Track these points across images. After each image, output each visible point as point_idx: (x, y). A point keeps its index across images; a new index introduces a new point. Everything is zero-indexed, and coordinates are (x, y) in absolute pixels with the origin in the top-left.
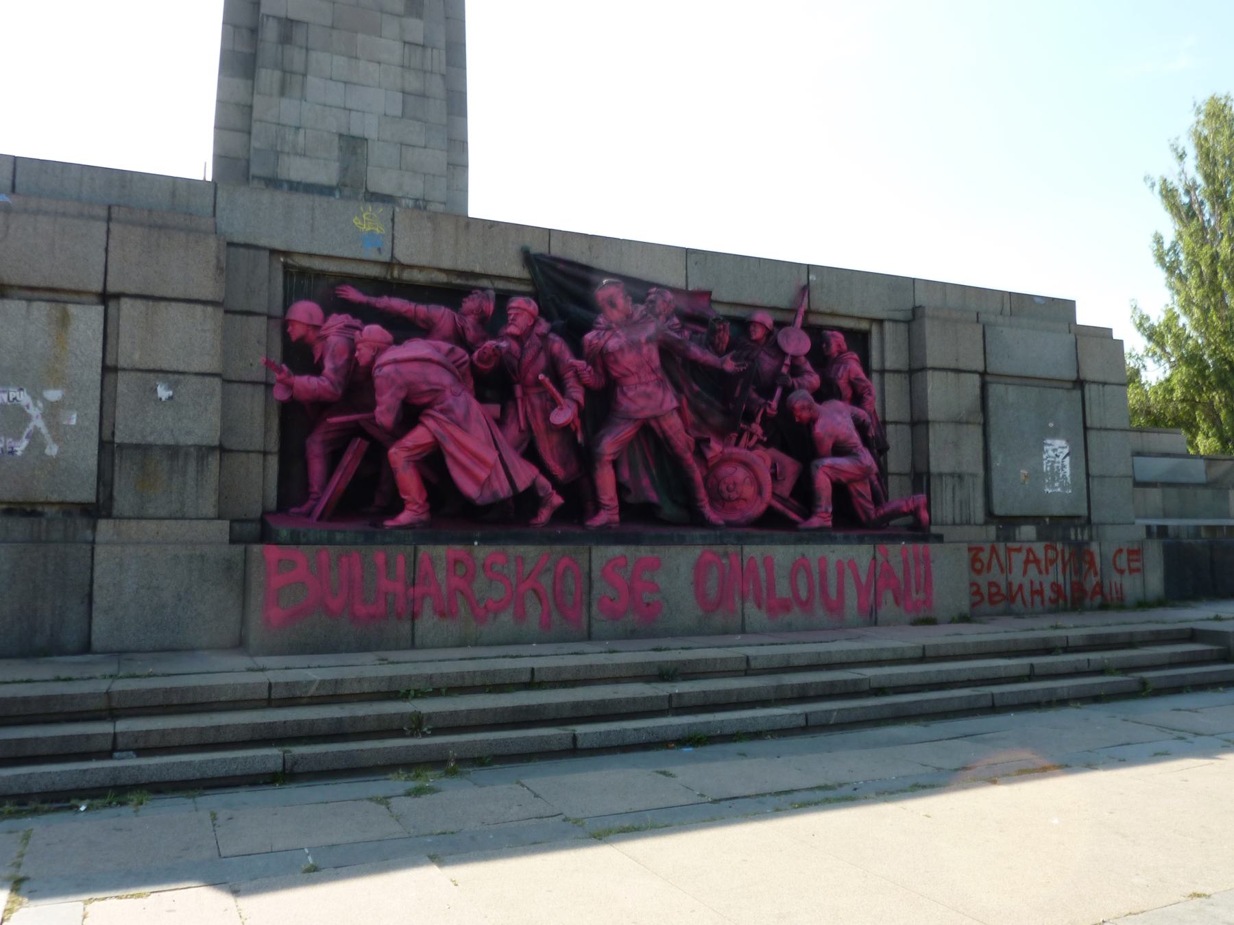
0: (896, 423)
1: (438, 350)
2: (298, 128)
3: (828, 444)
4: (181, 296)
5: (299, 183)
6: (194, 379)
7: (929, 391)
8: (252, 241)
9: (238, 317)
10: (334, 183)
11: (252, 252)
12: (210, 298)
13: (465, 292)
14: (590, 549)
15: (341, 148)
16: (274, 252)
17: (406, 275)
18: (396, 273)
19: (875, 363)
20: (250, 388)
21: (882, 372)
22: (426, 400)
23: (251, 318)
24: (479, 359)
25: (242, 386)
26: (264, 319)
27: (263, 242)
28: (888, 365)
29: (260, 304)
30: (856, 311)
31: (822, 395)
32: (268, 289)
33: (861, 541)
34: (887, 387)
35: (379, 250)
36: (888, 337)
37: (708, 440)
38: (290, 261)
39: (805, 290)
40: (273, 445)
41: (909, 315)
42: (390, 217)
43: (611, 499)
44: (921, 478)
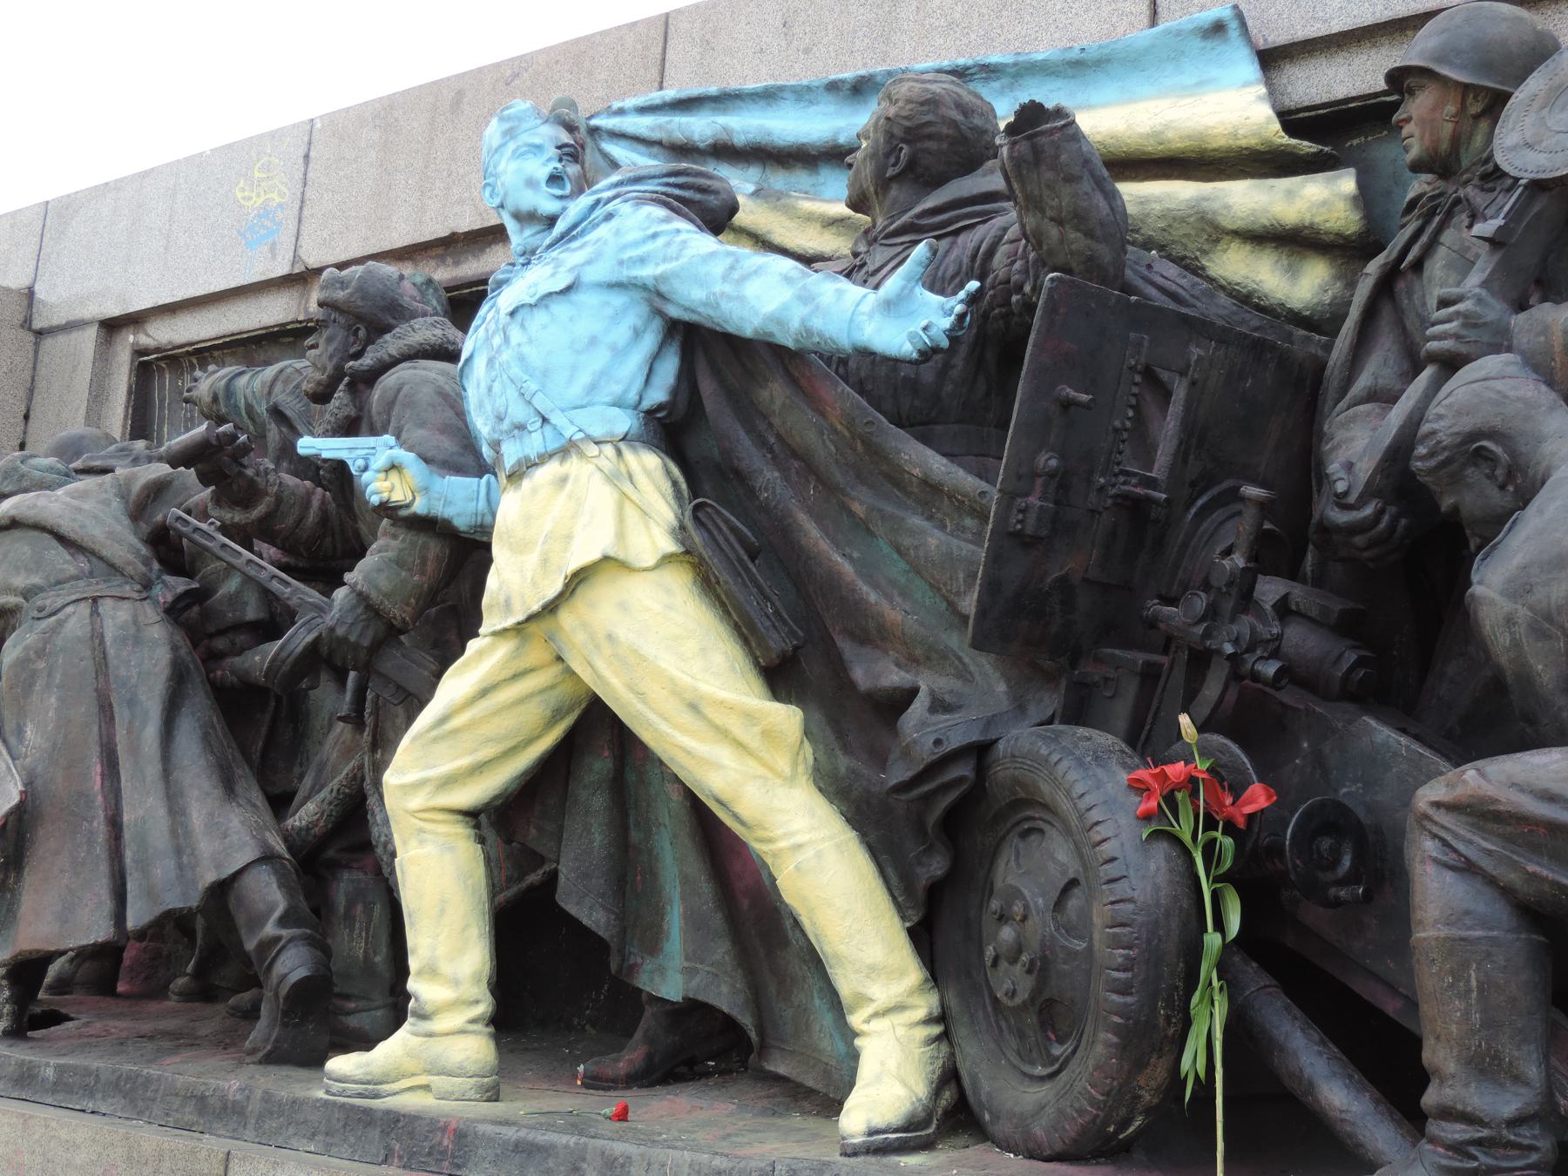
38: (144, 340)
42: (301, 152)
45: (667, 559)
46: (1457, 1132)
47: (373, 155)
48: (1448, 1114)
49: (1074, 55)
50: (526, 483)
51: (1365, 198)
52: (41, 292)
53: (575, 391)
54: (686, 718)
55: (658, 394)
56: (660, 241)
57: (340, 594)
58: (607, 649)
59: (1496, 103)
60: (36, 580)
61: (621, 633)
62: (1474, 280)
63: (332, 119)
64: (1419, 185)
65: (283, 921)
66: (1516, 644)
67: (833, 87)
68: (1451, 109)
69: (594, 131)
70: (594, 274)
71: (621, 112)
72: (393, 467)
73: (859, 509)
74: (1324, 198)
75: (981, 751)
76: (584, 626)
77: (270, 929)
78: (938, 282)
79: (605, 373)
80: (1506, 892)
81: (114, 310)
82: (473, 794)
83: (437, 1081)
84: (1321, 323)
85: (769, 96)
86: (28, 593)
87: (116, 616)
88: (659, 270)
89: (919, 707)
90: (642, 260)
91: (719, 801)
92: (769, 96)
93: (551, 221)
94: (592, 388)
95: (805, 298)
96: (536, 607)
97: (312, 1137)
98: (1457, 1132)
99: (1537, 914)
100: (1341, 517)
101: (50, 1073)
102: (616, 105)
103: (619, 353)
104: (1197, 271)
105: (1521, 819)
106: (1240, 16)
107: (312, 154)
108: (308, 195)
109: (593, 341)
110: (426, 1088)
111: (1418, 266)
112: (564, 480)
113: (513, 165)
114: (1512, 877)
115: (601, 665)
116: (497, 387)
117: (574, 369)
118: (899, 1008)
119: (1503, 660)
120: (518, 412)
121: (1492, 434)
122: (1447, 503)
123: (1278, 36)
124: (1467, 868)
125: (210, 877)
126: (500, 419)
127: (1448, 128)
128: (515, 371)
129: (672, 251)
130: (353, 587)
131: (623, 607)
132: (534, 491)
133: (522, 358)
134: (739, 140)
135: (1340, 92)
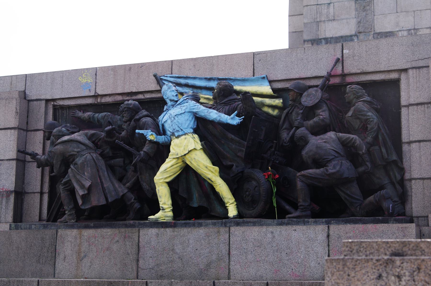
0: (419, 141)
2: (329, 4)
4: (3, 127)
5: (332, 38)
6: (6, 162)
8: (39, 98)
9: (33, 132)
10: (353, 33)
11: (38, 102)
12: (13, 126)
14: (139, 230)
15: (356, 10)
18: (99, 101)
23: (37, 132)
27: (43, 97)
28: (412, 101)
31: (320, 130)
32: (41, 118)
35: (90, 90)
36: (411, 80)
38: (55, 103)
40: (46, 189)
42: (95, 73)
45: (201, 149)
46: (301, 207)
47: (112, 76)
48: (301, 206)
49: (244, 79)
50: (180, 138)
51: (283, 103)
52: (27, 92)
53: (186, 126)
54: (205, 169)
55: (195, 127)
56: (196, 107)
57: (142, 153)
58: (194, 160)
59: (301, 95)
61: (196, 158)
62: (299, 117)
63: (101, 68)
64: (290, 102)
65: (134, 200)
67: (206, 79)
68: (295, 94)
69: (162, 79)
70: (187, 110)
71: (167, 77)
72: (152, 135)
73: (223, 142)
74: (278, 102)
75: (242, 172)
76: (190, 157)
77: (133, 201)
78: (238, 115)
79: (189, 124)
81: (50, 98)
82: (168, 180)
83: (166, 218)
84: (278, 117)
85: (195, 78)
86: (78, 152)
87: (94, 155)
88: (197, 110)
89: (234, 167)
90: (194, 109)
91: (209, 179)
92: (195, 78)
93: (177, 101)
94: (188, 126)
95: (219, 116)
96: (183, 155)
98: (301, 207)
99: (308, 185)
100: (286, 145)
101: (92, 225)
102: (166, 75)
103: (191, 121)
104: (261, 110)
105: (308, 176)
106: (267, 76)
107: (97, 74)
108: (97, 81)
109: (188, 120)
110: (164, 219)
111: (291, 113)
112: (186, 138)
113: (170, 93)
115: (193, 162)
116: (173, 125)
117: (186, 123)
118: (233, 203)
120: (178, 129)
121: (303, 137)
122: (298, 144)
123: (271, 79)
124: (302, 181)
125: (122, 194)
126: (174, 130)
128: (177, 123)
129: (198, 108)
130: (144, 151)
131: (196, 155)
132: (182, 140)
133: (178, 122)
134: (190, 84)
135: (280, 87)
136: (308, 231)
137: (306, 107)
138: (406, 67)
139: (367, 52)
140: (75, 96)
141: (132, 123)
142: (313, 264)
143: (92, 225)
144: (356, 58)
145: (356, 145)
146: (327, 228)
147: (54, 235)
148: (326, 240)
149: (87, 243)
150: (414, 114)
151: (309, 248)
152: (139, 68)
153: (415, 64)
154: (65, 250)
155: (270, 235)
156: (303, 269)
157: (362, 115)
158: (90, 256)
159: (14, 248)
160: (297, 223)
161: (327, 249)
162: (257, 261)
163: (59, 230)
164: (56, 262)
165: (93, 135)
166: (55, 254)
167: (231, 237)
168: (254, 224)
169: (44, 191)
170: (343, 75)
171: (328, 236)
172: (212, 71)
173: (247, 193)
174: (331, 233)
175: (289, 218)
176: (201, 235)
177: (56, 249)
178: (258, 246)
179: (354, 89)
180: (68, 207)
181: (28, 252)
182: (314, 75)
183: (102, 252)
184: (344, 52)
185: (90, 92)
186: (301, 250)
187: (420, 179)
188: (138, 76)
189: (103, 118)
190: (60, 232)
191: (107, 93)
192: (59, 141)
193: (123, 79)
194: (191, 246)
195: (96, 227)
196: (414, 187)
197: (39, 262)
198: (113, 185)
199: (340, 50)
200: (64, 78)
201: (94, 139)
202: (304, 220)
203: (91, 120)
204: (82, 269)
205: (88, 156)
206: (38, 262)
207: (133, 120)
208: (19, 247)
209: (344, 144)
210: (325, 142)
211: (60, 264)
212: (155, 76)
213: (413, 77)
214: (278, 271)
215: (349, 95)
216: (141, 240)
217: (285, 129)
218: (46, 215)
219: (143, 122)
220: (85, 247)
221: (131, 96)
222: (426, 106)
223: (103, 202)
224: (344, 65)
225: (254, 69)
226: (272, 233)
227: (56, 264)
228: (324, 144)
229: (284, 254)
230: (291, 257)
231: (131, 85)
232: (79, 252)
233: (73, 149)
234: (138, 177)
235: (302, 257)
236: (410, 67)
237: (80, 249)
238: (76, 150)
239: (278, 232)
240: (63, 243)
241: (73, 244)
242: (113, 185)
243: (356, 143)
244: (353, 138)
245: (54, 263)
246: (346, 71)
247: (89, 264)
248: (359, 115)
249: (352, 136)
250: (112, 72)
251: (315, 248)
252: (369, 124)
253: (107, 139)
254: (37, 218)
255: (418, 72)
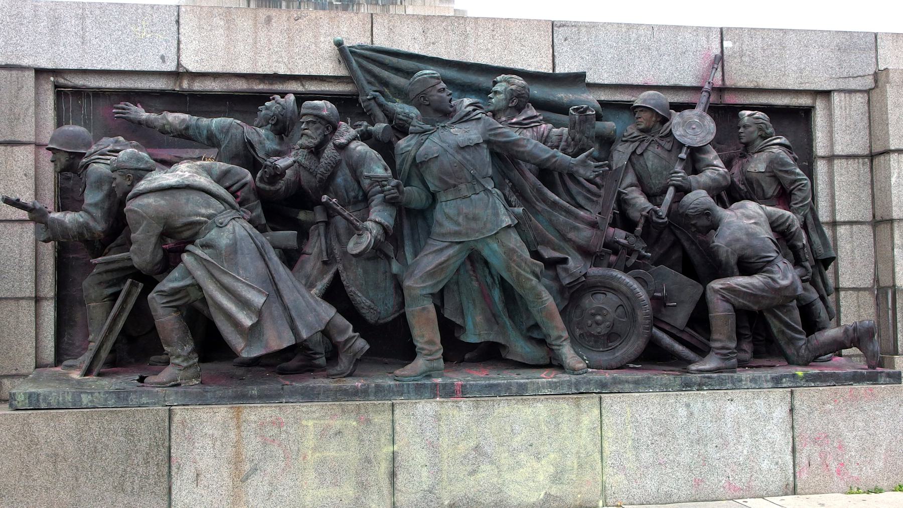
0: (851, 223)
1: (209, 172)
3: (733, 261)
7: (893, 180)
8: (15, 61)
11: (14, 73)
13: (264, 97)
16: (40, 72)
17: (198, 86)
18: (185, 85)
19: (820, 147)
20: (17, 227)
21: (831, 158)
22: (187, 234)
23: (16, 148)
24: (261, 179)
25: (9, 225)
26: (31, 148)
27: (25, 62)
28: (838, 150)
29: (26, 132)
30: (791, 84)
33: (777, 382)
34: (837, 178)
36: (837, 112)
37: (564, 261)
38: (61, 81)
39: (720, 59)
40: (49, 289)
41: (869, 83)
42: (174, 18)
43: (431, 342)
44: (884, 292)
47: (221, 31)
60: (211, 211)
66: (727, 256)
68: (654, 119)
75: (585, 275)
80: (733, 306)
86: (210, 217)
97: (401, 395)
100: (661, 221)
105: (740, 291)
107: (181, 21)
108: (182, 38)
114: (736, 303)
119: (723, 259)
124: (727, 301)
125: (328, 319)
127: (652, 124)
130: (376, 222)
136: (756, 401)
137: (689, 147)
138: (829, 88)
139: (762, 48)
140: (122, 68)
141: (329, 152)
142: (765, 465)
143: (255, 392)
144: (746, 59)
145: (793, 229)
146: (789, 395)
147: (164, 421)
148: (789, 419)
149: (258, 439)
150: (841, 175)
151: (757, 434)
152: (292, 20)
153: (842, 85)
154: (198, 458)
155: (683, 412)
156: (749, 475)
157: (786, 172)
158: (269, 470)
159: (43, 458)
160: (721, 385)
161: (790, 435)
162: (660, 464)
163: (177, 410)
164: (174, 487)
165: (226, 173)
166: (170, 467)
167: (603, 418)
168: (638, 386)
169: (42, 295)
170: (721, 90)
171: (792, 410)
172: (464, 48)
173: (599, 318)
174: (797, 403)
175: (701, 371)
176: (538, 415)
177: (170, 457)
178: (661, 434)
179: (761, 121)
180: (183, 349)
181: (87, 466)
182: (672, 82)
183: (301, 459)
184: (725, 46)
185: (164, 61)
186: (744, 440)
187: (853, 289)
188: (291, 39)
189: (226, 130)
190: (180, 413)
191: (210, 71)
192: (143, 185)
193: (250, 40)
194: (519, 439)
195: (265, 398)
196: (843, 303)
197: (123, 490)
198: (303, 297)
199: (718, 40)
200: (88, 21)
201: (227, 184)
202: (732, 377)
203: (191, 132)
204: (247, 502)
205: (234, 230)
206: (120, 488)
207: (330, 145)
208: (56, 455)
209: (776, 226)
210: (755, 223)
211: (184, 493)
212: (339, 44)
213: (841, 108)
214: (702, 481)
215: (751, 129)
216: (398, 428)
217: (631, 185)
218: (53, 353)
219: (360, 152)
220: (252, 446)
221: (272, 84)
222: (861, 160)
223: (288, 340)
224: (725, 71)
225: (553, 55)
226: (688, 405)
227: (174, 493)
228: (758, 229)
229: (711, 449)
230: (725, 453)
231: (274, 57)
232: (237, 461)
233: (196, 208)
234: (337, 275)
235: (745, 452)
236: (835, 88)
237: (238, 454)
238: (203, 211)
239: (699, 405)
240: (190, 440)
241: (218, 443)
242: (303, 297)
243: (793, 226)
244: (789, 217)
245: (166, 491)
246: (729, 83)
247: (267, 488)
248: (781, 171)
249: (788, 213)
250: (222, 23)
251: (769, 435)
252: (800, 190)
253: (262, 186)
254: (31, 361)
255: (848, 98)
